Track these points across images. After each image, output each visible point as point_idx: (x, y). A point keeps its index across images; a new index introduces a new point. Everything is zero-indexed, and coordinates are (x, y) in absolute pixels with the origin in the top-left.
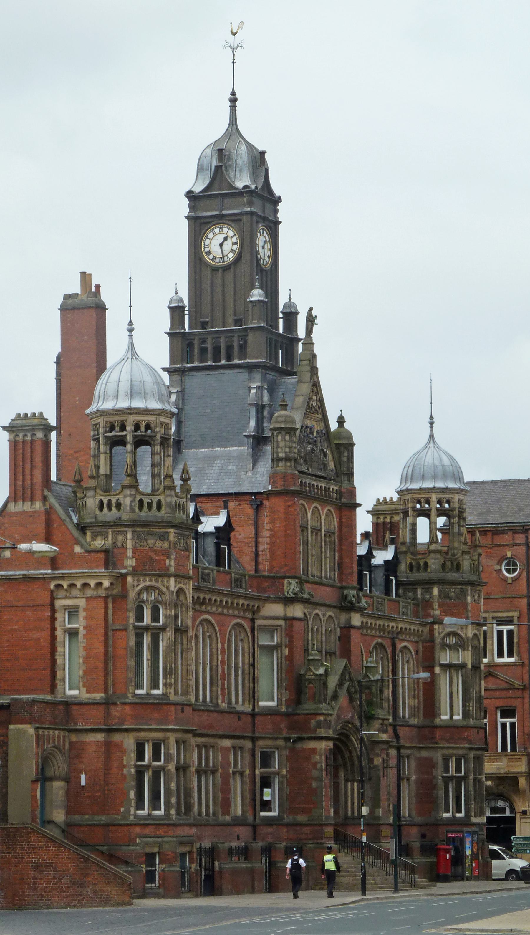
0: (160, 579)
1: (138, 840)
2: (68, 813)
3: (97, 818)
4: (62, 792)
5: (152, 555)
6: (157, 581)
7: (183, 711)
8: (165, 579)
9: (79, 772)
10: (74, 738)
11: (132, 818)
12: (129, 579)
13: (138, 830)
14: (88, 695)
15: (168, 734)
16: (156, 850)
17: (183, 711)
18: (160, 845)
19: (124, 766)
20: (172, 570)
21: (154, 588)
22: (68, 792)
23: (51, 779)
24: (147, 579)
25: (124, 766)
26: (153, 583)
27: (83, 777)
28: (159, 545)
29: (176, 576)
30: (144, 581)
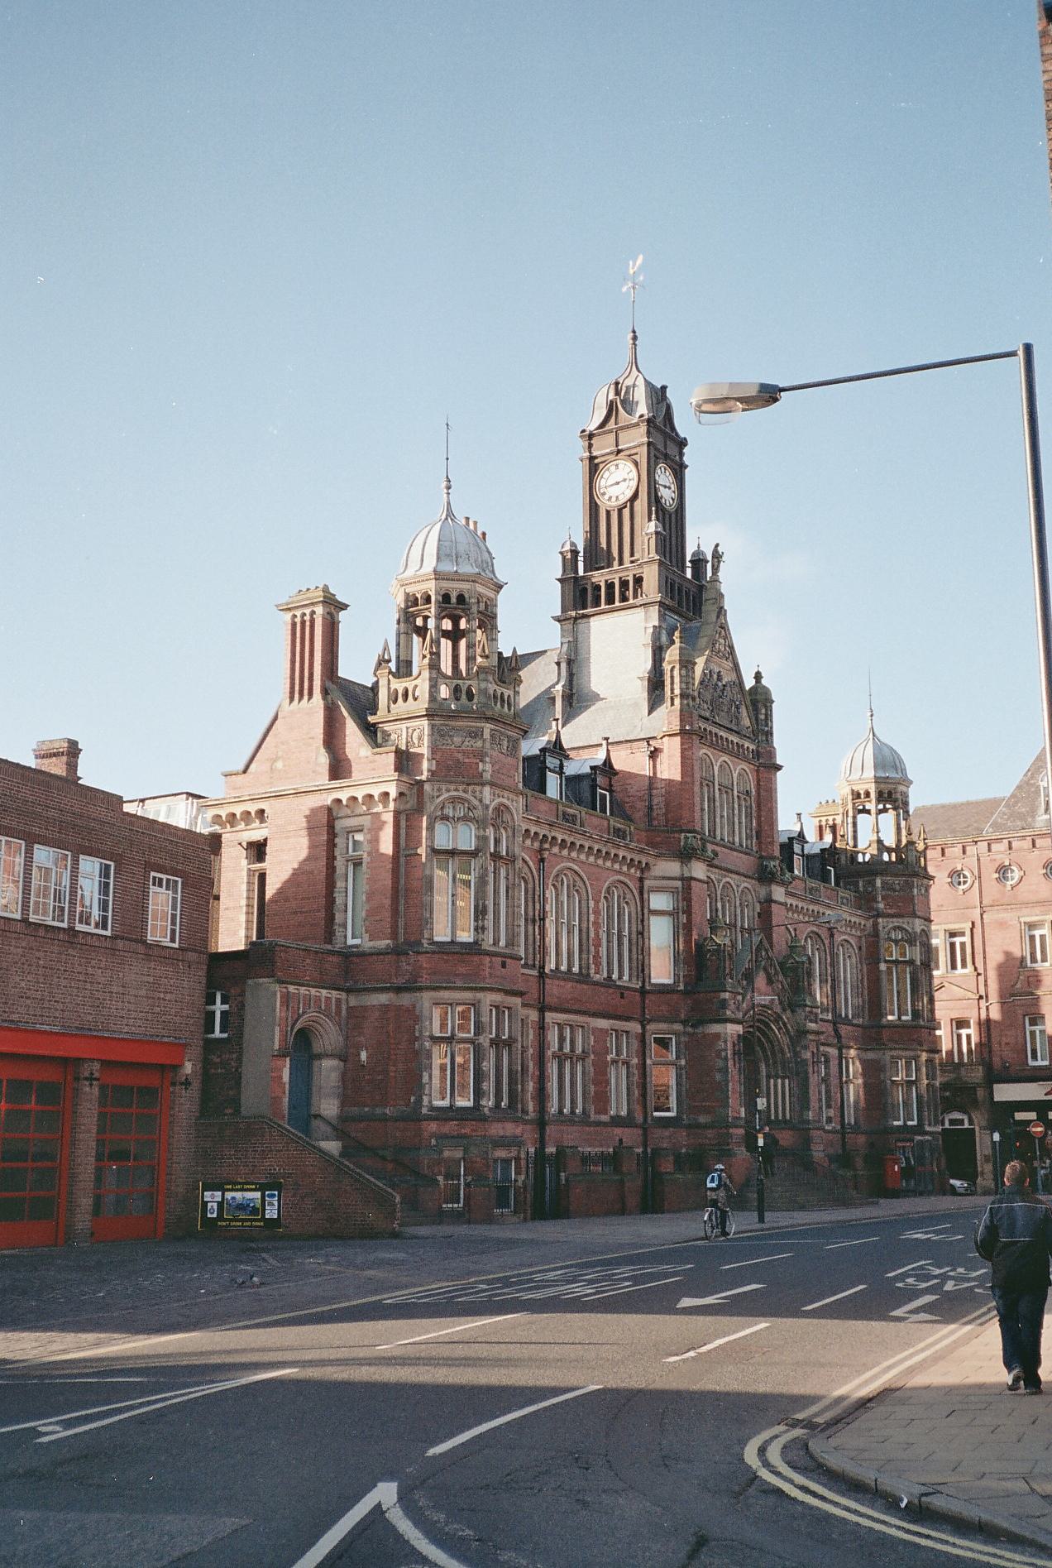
0: (470, 788)
1: (433, 1142)
2: (343, 1104)
3: (379, 1111)
4: (334, 1077)
5: (460, 756)
6: (465, 791)
7: (504, 965)
8: (478, 788)
9: (359, 1047)
10: (353, 1001)
11: (424, 1111)
12: (427, 787)
13: (433, 1127)
14: (371, 944)
15: (480, 995)
16: (459, 1154)
17: (504, 965)
18: (466, 1151)
19: (417, 1039)
20: (487, 776)
21: (461, 800)
22: (344, 1075)
23: (320, 1057)
24: (452, 787)
25: (417, 1039)
26: (461, 794)
27: (364, 1055)
28: (469, 743)
29: (492, 784)
30: (448, 791)
